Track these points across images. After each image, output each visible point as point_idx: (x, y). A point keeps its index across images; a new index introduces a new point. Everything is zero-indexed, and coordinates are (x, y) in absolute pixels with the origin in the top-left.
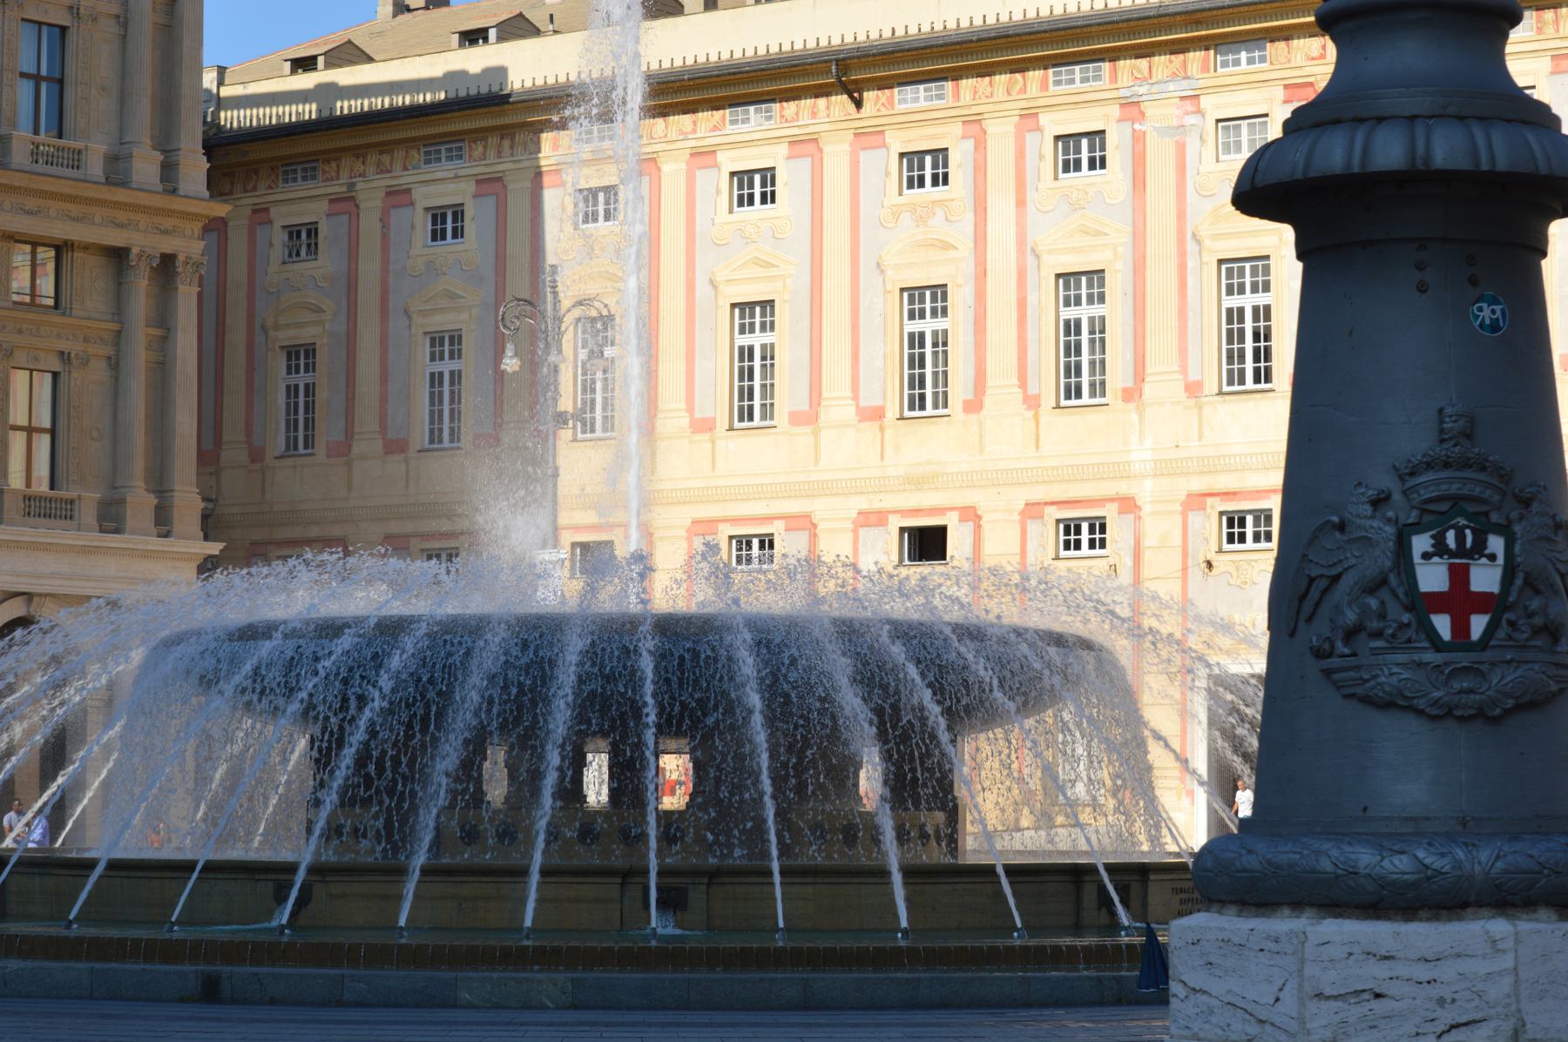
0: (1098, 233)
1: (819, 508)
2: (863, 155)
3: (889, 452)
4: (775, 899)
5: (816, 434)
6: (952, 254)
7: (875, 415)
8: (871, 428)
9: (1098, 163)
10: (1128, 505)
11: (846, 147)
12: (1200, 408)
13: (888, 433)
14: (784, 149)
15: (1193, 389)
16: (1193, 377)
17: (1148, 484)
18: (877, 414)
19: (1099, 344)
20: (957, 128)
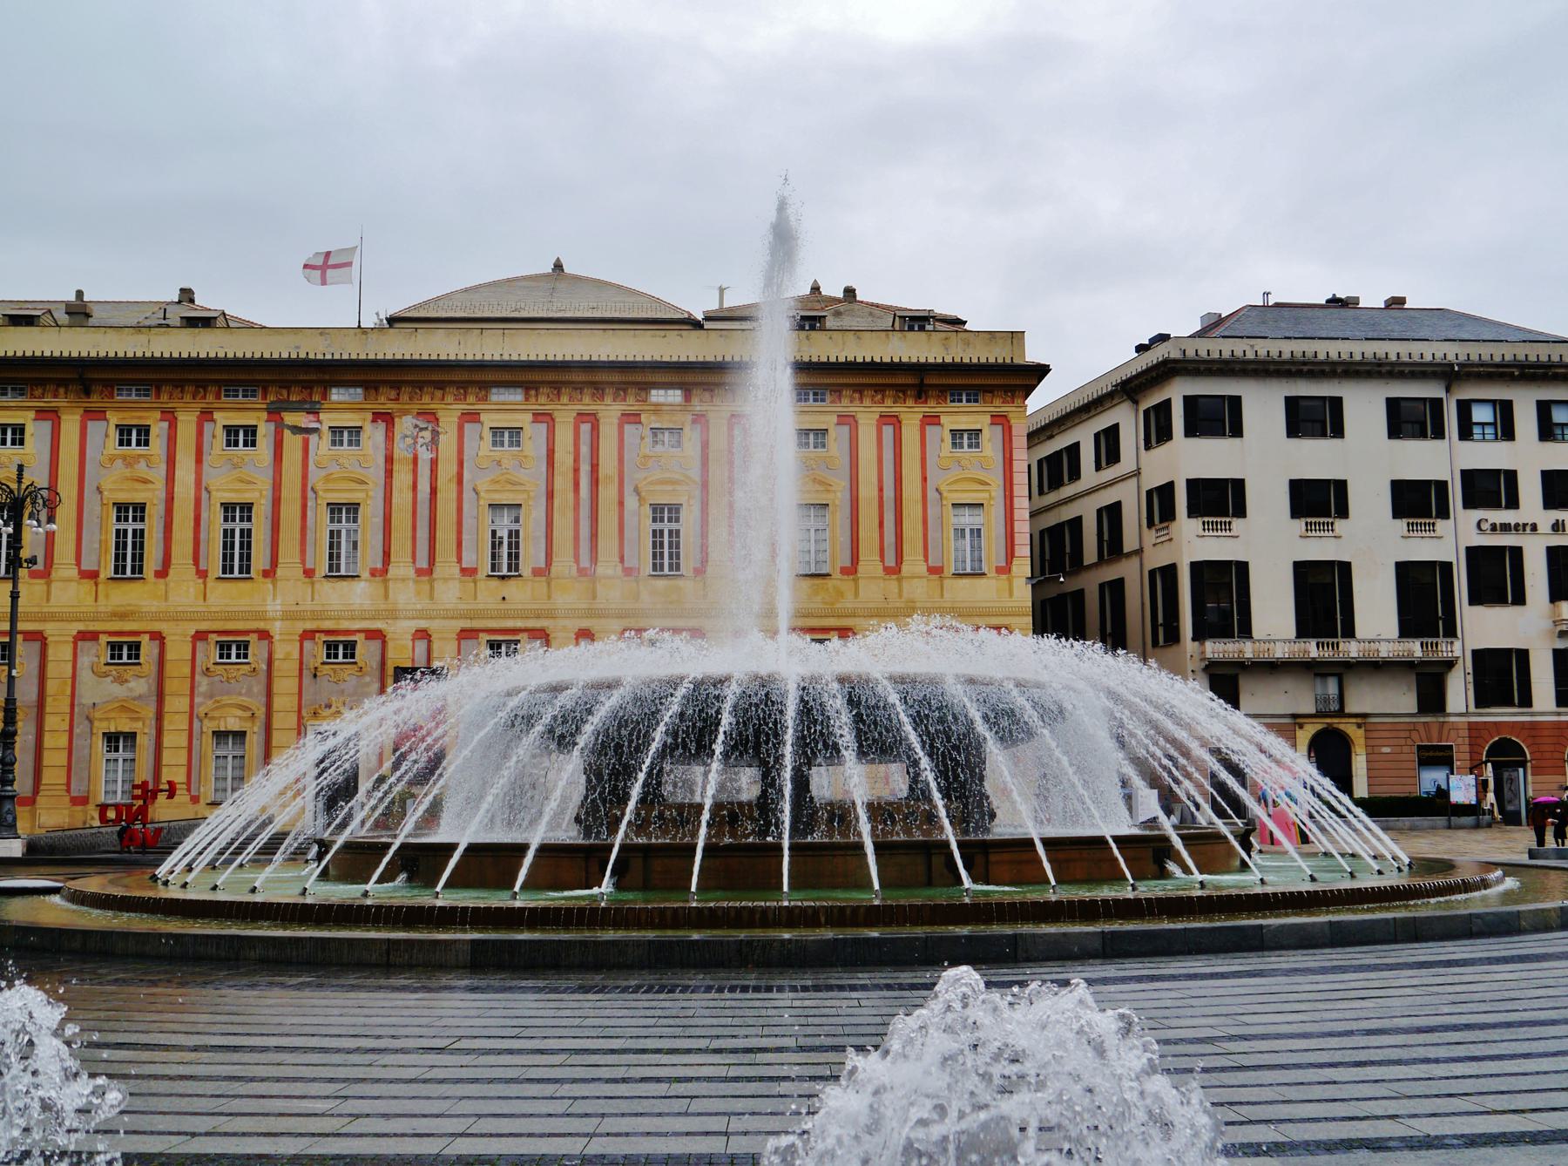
0: (250, 482)
1: (49, 628)
2: (90, 424)
3: (101, 597)
4: (1050, 861)
5: (49, 585)
6: (150, 486)
7: (93, 575)
8: (88, 585)
9: (251, 443)
10: (265, 635)
11: (77, 417)
12: (313, 584)
13: (101, 587)
14: (32, 414)
15: (309, 573)
16: (309, 565)
17: (278, 624)
18: (93, 575)
19: (246, 545)
20: (158, 415)
